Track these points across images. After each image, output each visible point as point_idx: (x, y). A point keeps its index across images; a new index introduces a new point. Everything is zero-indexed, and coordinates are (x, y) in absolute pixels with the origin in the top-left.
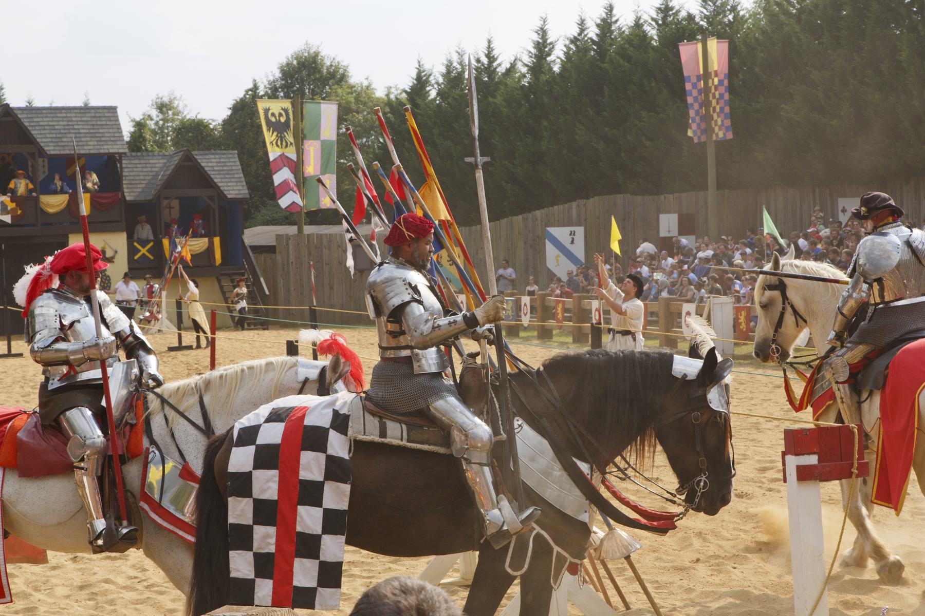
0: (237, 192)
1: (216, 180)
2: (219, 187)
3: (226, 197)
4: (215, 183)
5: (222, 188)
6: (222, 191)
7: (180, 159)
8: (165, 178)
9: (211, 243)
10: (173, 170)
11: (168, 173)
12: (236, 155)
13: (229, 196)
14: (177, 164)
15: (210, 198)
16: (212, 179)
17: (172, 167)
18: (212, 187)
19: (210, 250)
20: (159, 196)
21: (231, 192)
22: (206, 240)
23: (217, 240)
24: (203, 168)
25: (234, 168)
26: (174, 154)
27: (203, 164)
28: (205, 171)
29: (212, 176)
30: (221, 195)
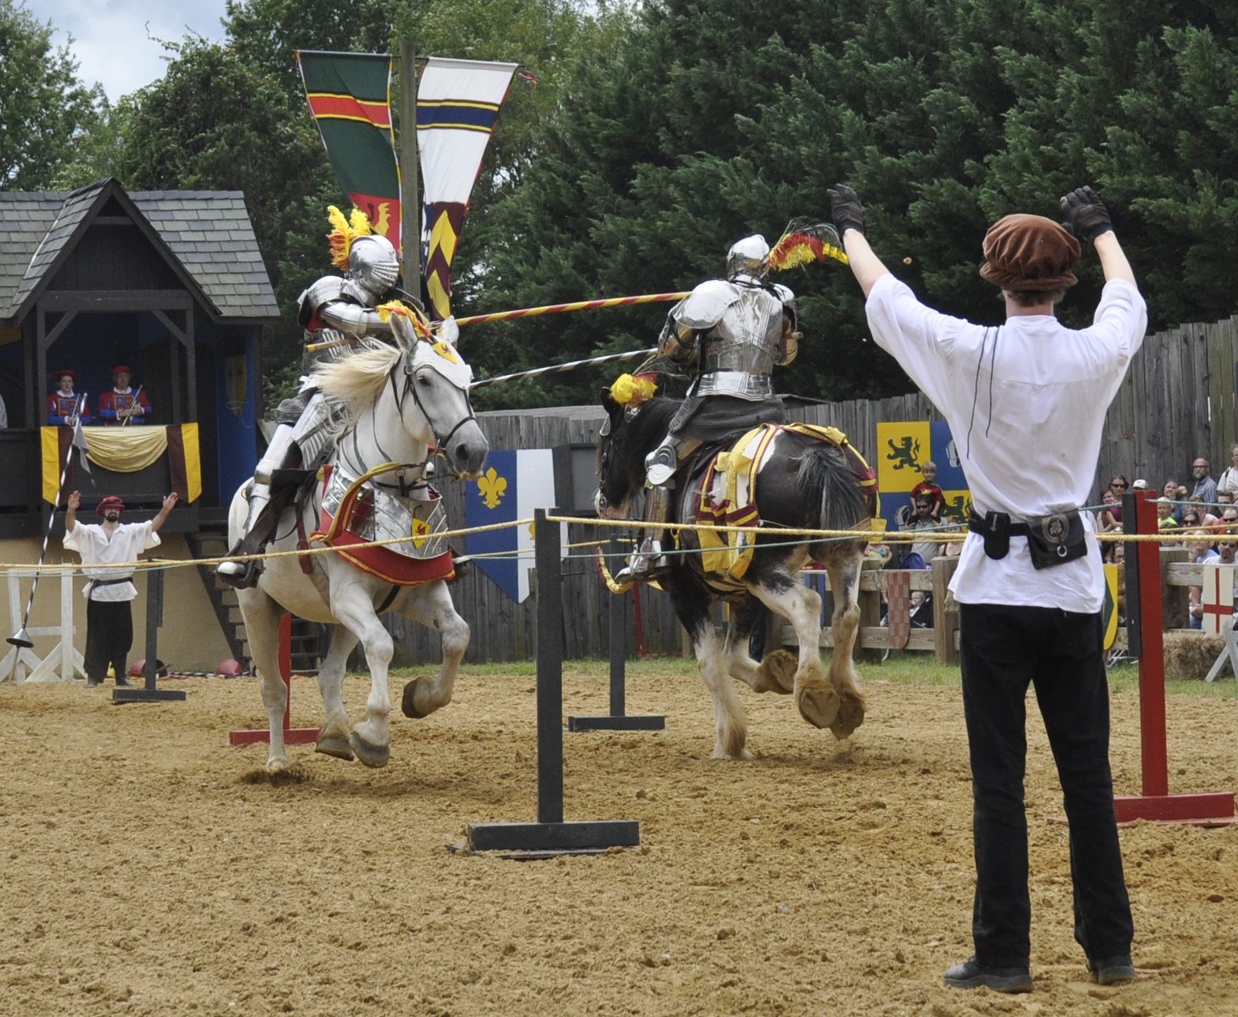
0: (247, 301)
1: (188, 268)
2: (197, 287)
3: (217, 312)
4: (188, 276)
5: (206, 290)
6: (206, 299)
7: (90, 208)
8: (51, 258)
9: (175, 441)
10: (73, 236)
11: (59, 244)
12: (242, 204)
13: (226, 312)
14: (82, 222)
15: (177, 316)
16: (172, 255)
17: (72, 229)
18: (180, 286)
19: (172, 457)
20: (34, 309)
21: (231, 301)
22: (161, 430)
23: (190, 434)
24: (156, 234)
25: (235, 236)
26: (73, 197)
27: (157, 226)
28: (163, 244)
29: (181, 258)
30: (203, 306)
